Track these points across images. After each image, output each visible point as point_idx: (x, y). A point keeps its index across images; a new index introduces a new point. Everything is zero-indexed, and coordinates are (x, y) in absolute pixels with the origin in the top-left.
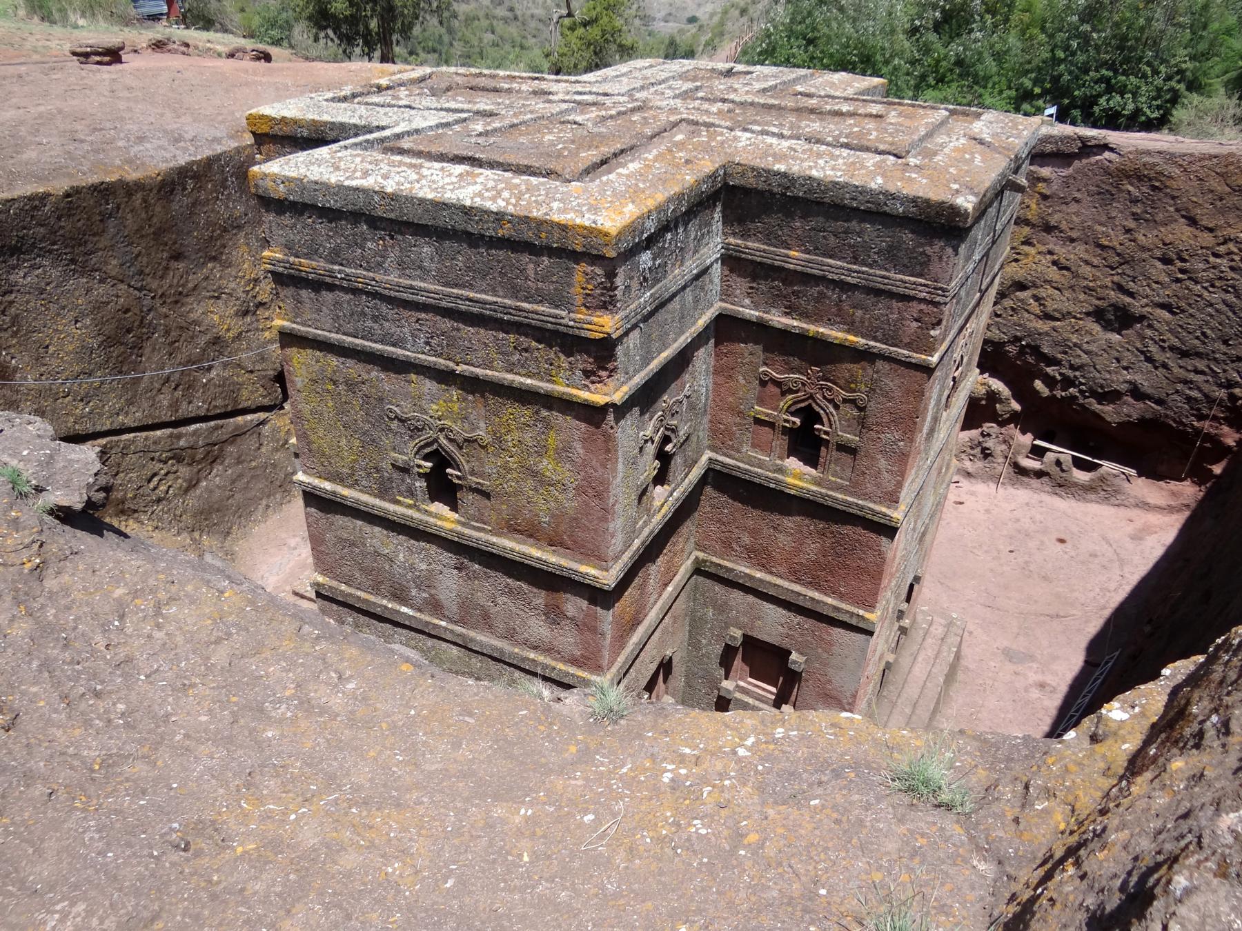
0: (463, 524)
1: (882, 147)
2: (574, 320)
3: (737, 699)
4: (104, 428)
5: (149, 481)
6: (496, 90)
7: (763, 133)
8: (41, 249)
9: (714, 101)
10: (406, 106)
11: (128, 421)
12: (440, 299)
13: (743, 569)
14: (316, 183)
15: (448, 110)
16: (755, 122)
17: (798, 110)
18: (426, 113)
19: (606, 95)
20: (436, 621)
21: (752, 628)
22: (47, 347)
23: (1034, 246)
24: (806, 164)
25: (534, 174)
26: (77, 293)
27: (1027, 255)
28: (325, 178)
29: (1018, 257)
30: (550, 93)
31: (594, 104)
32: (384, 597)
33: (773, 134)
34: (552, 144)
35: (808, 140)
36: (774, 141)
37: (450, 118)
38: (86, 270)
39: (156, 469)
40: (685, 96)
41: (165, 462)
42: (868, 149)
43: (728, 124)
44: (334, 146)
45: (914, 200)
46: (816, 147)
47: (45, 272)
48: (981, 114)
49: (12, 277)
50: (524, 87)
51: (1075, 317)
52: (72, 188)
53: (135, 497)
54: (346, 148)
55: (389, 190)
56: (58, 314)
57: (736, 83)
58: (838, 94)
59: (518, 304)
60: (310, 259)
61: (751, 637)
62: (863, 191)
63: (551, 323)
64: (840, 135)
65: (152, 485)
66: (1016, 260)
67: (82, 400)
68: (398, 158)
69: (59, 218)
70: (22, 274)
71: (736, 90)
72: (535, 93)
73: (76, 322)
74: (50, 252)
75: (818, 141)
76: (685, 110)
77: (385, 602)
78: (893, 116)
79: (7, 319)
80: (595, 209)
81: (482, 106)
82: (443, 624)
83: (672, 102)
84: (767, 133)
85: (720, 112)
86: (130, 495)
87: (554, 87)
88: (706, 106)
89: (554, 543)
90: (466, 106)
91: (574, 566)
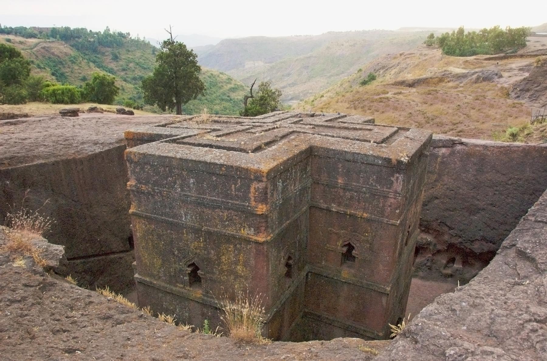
7: (326, 135)
9: (307, 125)
10: (186, 128)
16: (323, 132)
17: (340, 128)
18: (194, 130)
19: (264, 123)
30: (243, 123)
33: (330, 136)
36: (330, 138)
40: (295, 123)
46: (346, 140)
76: (295, 128)
84: (327, 135)
87: (245, 120)
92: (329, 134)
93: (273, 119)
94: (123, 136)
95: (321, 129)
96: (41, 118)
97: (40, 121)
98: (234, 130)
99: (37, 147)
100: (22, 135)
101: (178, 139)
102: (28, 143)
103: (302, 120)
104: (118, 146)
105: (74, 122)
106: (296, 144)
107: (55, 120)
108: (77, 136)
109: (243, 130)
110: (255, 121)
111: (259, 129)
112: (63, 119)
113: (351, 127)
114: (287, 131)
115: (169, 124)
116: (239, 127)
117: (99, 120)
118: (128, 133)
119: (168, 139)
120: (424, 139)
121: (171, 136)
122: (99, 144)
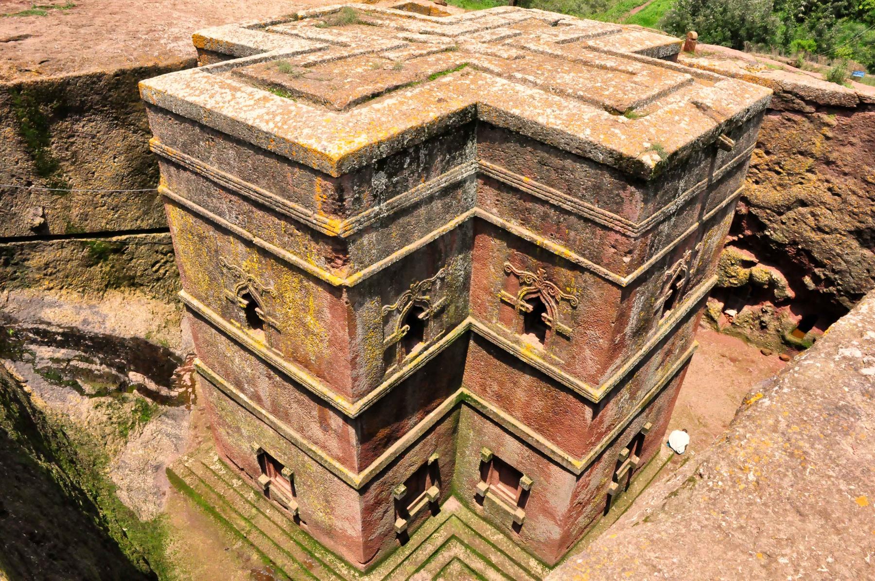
3: (489, 499)
4: (127, 228)
5: (153, 266)
8: (95, 109)
11: (144, 225)
13: (493, 408)
21: (498, 451)
22: (93, 173)
23: (816, 174)
26: (117, 139)
27: (809, 180)
29: (802, 181)
38: (125, 124)
39: (159, 258)
41: (165, 254)
47: (96, 125)
49: (75, 127)
52: (121, 70)
53: (142, 275)
56: (103, 152)
61: (497, 457)
65: (154, 269)
66: (801, 183)
67: (113, 209)
69: (109, 90)
70: (81, 124)
73: (115, 158)
74: (102, 111)
79: (69, 153)
86: (139, 274)
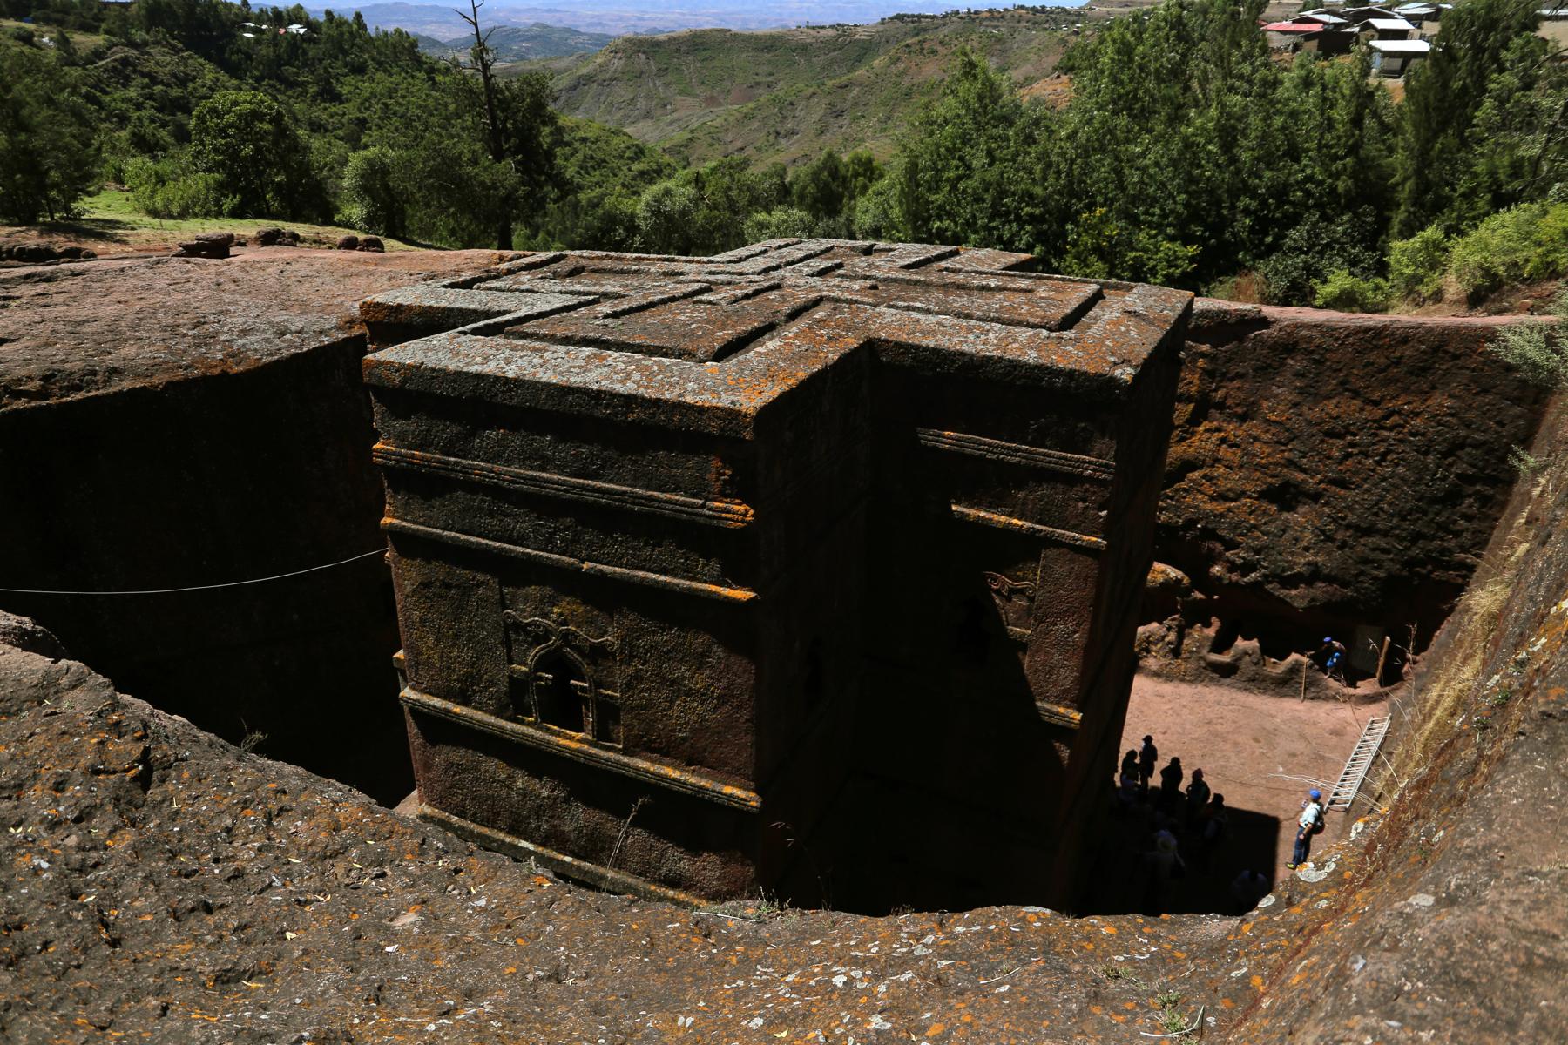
0: (590, 743)
1: (1032, 320)
2: (710, 509)
6: (622, 272)
7: (908, 308)
9: (855, 278)
10: (528, 291)
12: (565, 491)
14: (433, 370)
15: (572, 293)
16: (899, 298)
17: (945, 287)
18: (549, 297)
19: (741, 274)
20: (561, 857)
24: (956, 339)
25: (666, 355)
28: (442, 365)
30: (682, 274)
31: (729, 283)
32: (501, 830)
33: (919, 310)
34: (685, 324)
35: (958, 315)
36: (921, 316)
37: (574, 300)
40: (822, 273)
42: (1019, 323)
43: (871, 300)
44: (453, 332)
45: (1071, 374)
46: (964, 323)
48: (1132, 288)
50: (653, 269)
51: (1250, 497)
54: (464, 333)
55: (511, 375)
57: (878, 260)
58: (985, 269)
59: (650, 493)
60: (424, 451)
62: (1015, 365)
63: (687, 513)
64: (990, 311)
68: (521, 342)
71: (877, 267)
72: (666, 274)
75: (968, 316)
76: (824, 287)
77: (501, 836)
78: (1042, 291)
80: (733, 390)
81: (609, 289)
82: (568, 859)
83: (811, 280)
85: (862, 290)
87: (686, 268)
88: (846, 284)
89: (691, 760)
90: (592, 289)
91: (719, 787)
92: (918, 304)
93: (761, 263)
94: (356, 310)
95: (893, 288)
96: (126, 263)
97: (122, 270)
98: (660, 297)
99: (118, 340)
100: (76, 312)
101: (509, 323)
102: (93, 334)
103: (840, 266)
104: (344, 339)
105: (219, 274)
106: (831, 333)
107: (165, 268)
108: (228, 312)
109: (686, 296)
110: (711, 267)
111: (728, 293)
112: (189, 266)
113: (976, 283)
114: (803, 297)
115: (480, 280)
116: (672, 288)
117: (288, 267)
118: (367, 308)
119: (481, 324)
120: (1172, 315)
121: (488, 314)
122: (292, 333)
